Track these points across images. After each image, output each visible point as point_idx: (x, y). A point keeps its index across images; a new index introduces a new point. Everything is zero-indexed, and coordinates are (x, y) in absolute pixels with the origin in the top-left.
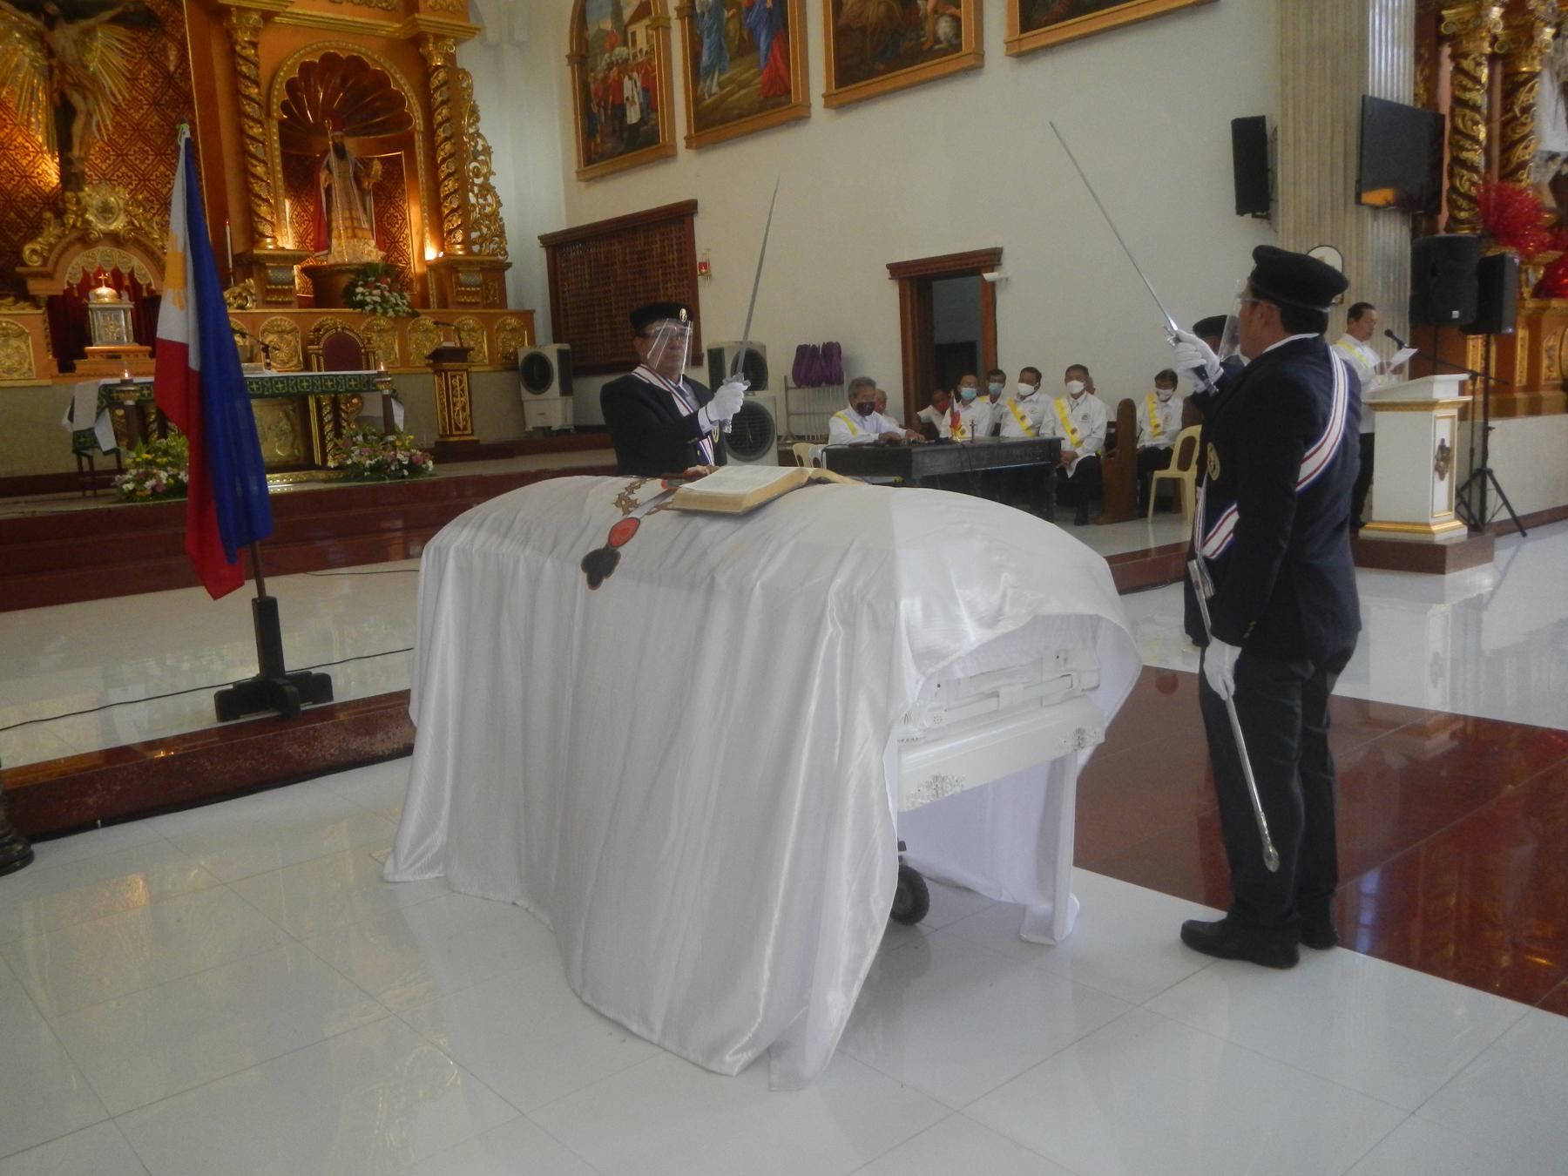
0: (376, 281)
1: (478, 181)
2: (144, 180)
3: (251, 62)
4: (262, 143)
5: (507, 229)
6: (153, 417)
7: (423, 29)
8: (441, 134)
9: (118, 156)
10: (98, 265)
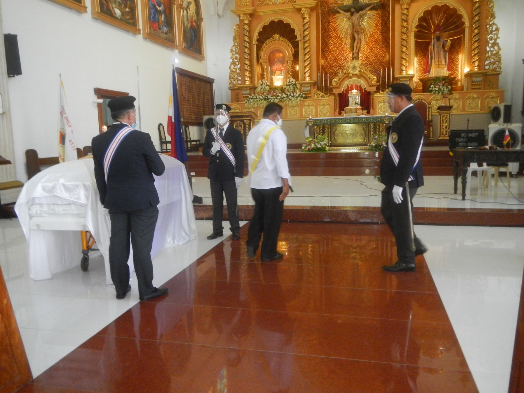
0: (438, 83)
1: (491, 42)
3: (405, 15)
5: (502, 59)
6: (321, 129)
8: (474, 26)
9: (370, 50)
10: (351, 84)
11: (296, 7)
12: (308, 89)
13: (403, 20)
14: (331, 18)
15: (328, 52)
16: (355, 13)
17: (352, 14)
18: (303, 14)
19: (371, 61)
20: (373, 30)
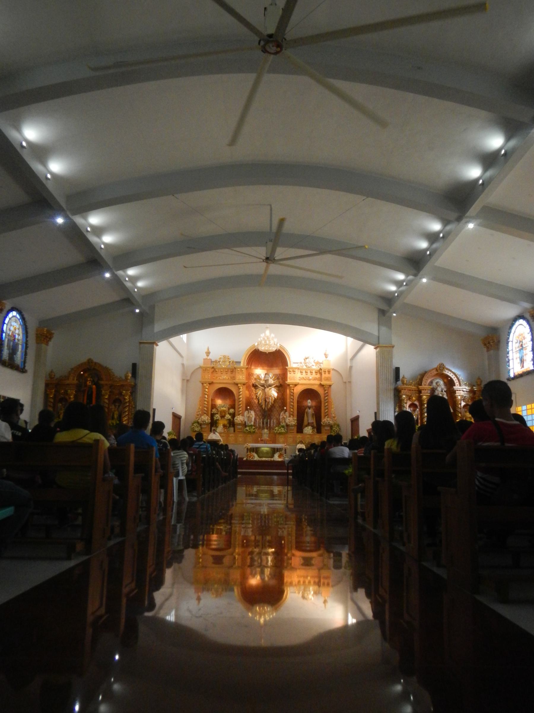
11: (236, 383)
12: (240, 427)
13: (291, 395)
17: (265, 388)
18: (239, 387)
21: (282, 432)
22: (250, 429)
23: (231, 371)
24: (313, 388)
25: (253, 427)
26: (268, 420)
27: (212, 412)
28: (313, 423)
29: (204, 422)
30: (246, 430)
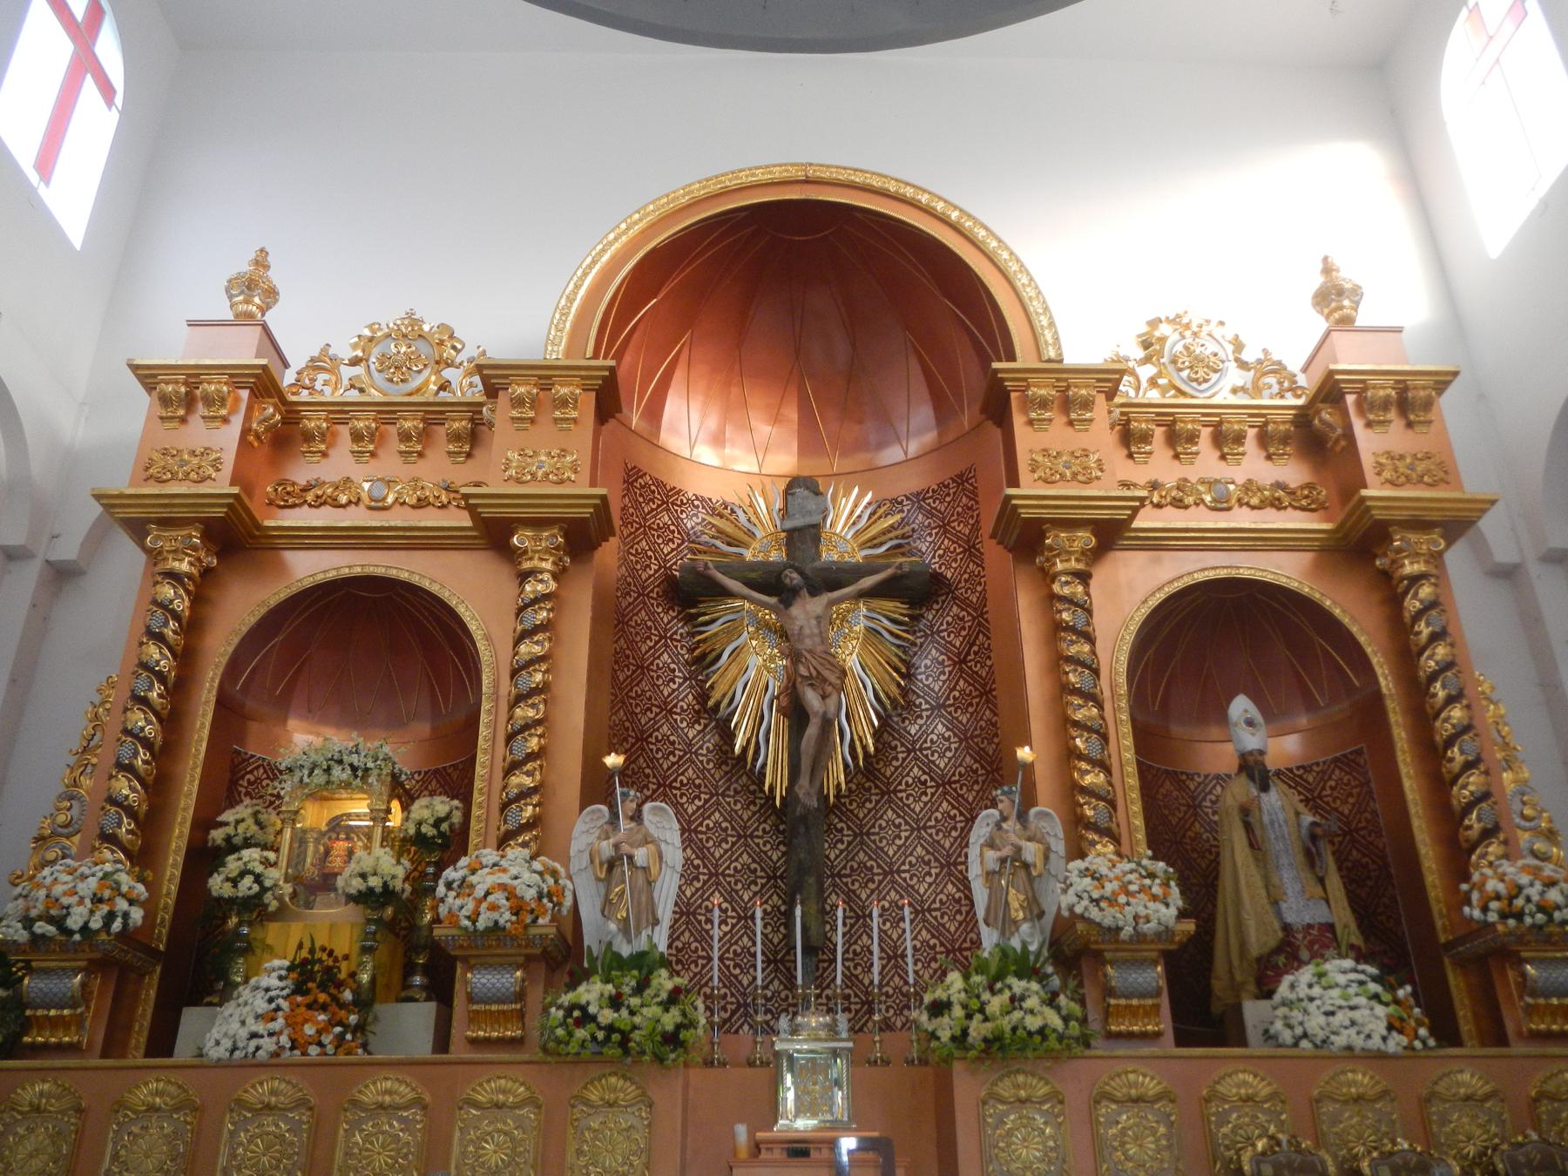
2: (919, 829)
3: (1077, 605)
4: (1097, 732)
7: (1378, 515)
9: (883, 794)
11: (486, 512)
12: (510, 980)
14: (673, 618)
15: (651, 786)
16: (804, 592)
19: (891, 853)
20: (894, 691)
21: (1033, 1023)
22: (615, 1002)
23: (455, 437)
24: (1269, 578)
25: (664, 982)
26: (826, 914)
27: (217, 835)
28: (1330, 927)
29: (41, 927)
30: (569, 1011)
